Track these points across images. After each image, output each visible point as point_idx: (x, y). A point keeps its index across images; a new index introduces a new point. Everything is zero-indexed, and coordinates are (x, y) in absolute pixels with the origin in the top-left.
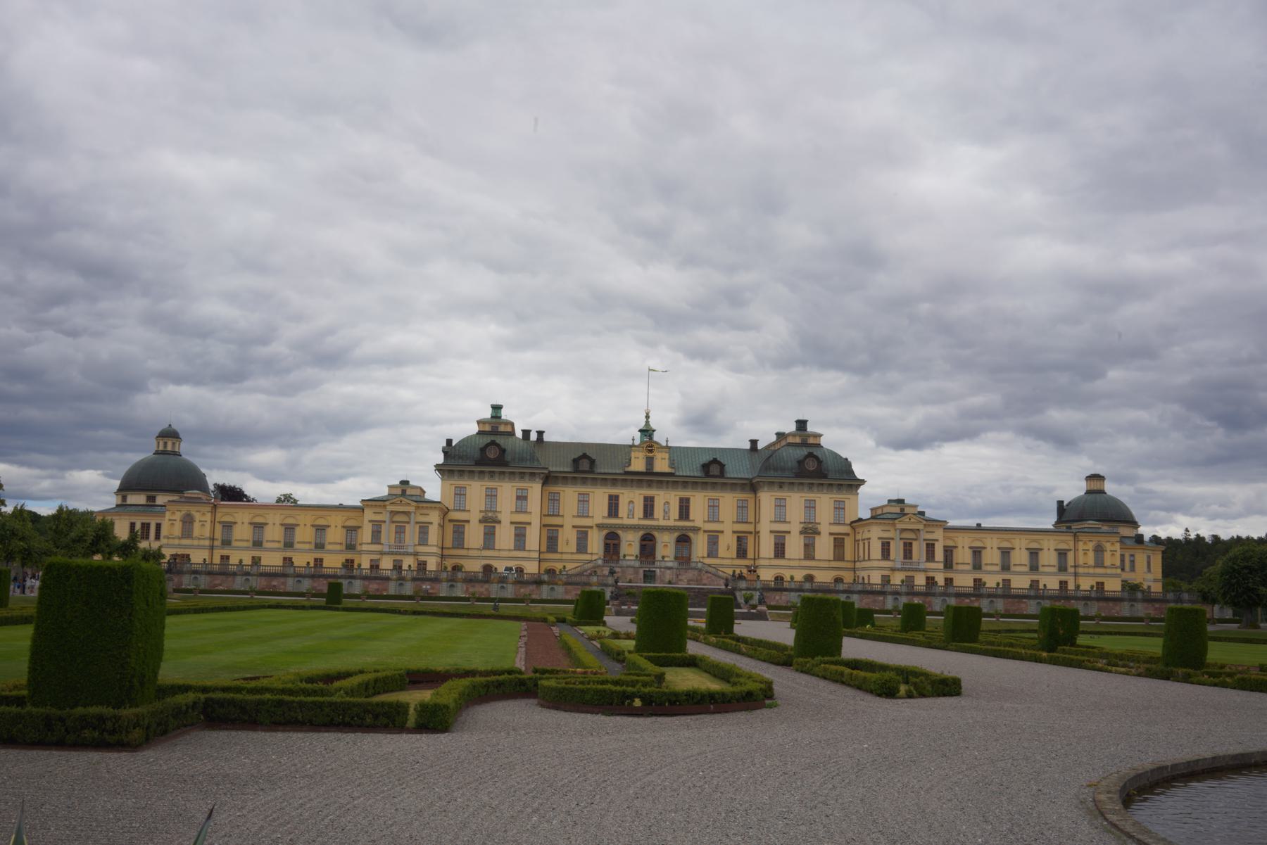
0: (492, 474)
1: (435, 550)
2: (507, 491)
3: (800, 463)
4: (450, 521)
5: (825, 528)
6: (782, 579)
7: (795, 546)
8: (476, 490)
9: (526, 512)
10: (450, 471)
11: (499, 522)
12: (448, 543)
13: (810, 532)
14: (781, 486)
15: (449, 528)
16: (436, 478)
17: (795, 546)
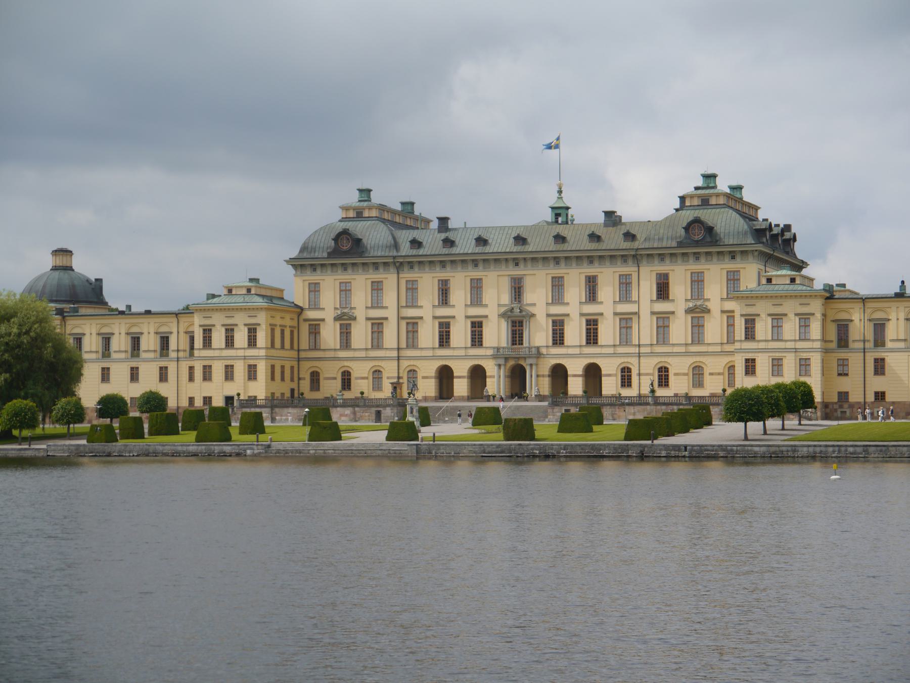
0: (345, 267)
1: (262, 353)
2: (360, 284)
3: (687, 229)
4: (306, 320)
5: (715, 305)
6: (667, 370)
7: (680, 329)
8: (329, 284)
9: (383, 307)
10: (302, 266)
11: (355, 319)
12: (304, 345)
13: (698, 312)
14: (662, 257)
15: (305, 329)
16: (290, 270)
17: (680, 329)
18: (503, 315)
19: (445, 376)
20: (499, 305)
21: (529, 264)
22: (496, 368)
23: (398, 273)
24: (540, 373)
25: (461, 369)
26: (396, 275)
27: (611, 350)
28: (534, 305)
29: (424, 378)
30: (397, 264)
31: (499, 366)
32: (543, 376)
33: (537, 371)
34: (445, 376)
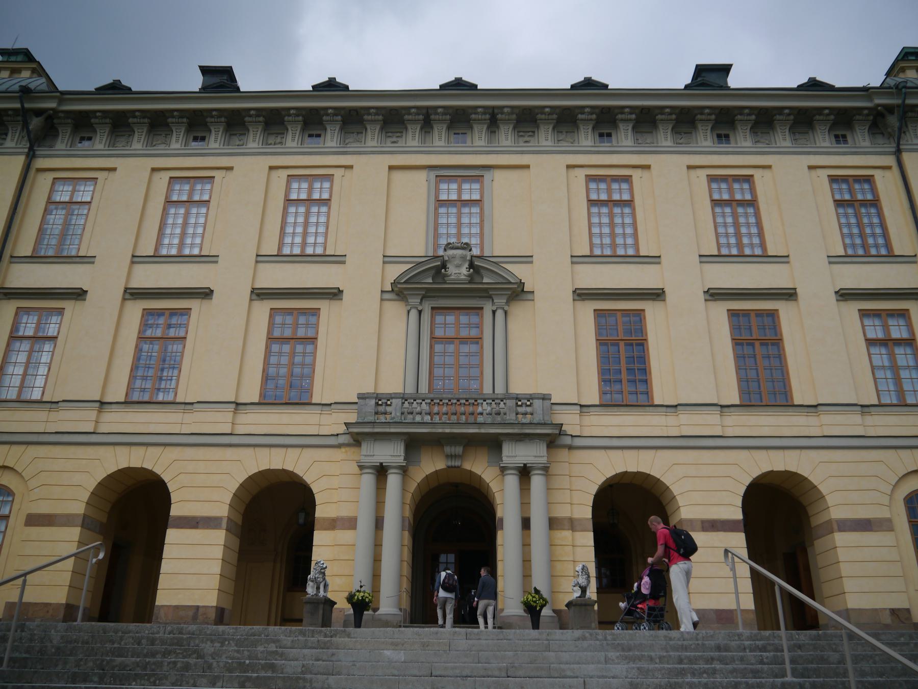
18: (400, 291)
19: (134, 514)
20: (388, 260)
21: (506, 137)
22: (368, 480)
23: (31, 156)
24: (563, 512)
25: (204, 487)
26: (20, 160)
27: (851, 423)
28: (527, 259)
29: (34, 520)
30: (35, 123)
31: (381, 472)
32: (573, 524)
33: (549, 504)
34: (134, 514)
